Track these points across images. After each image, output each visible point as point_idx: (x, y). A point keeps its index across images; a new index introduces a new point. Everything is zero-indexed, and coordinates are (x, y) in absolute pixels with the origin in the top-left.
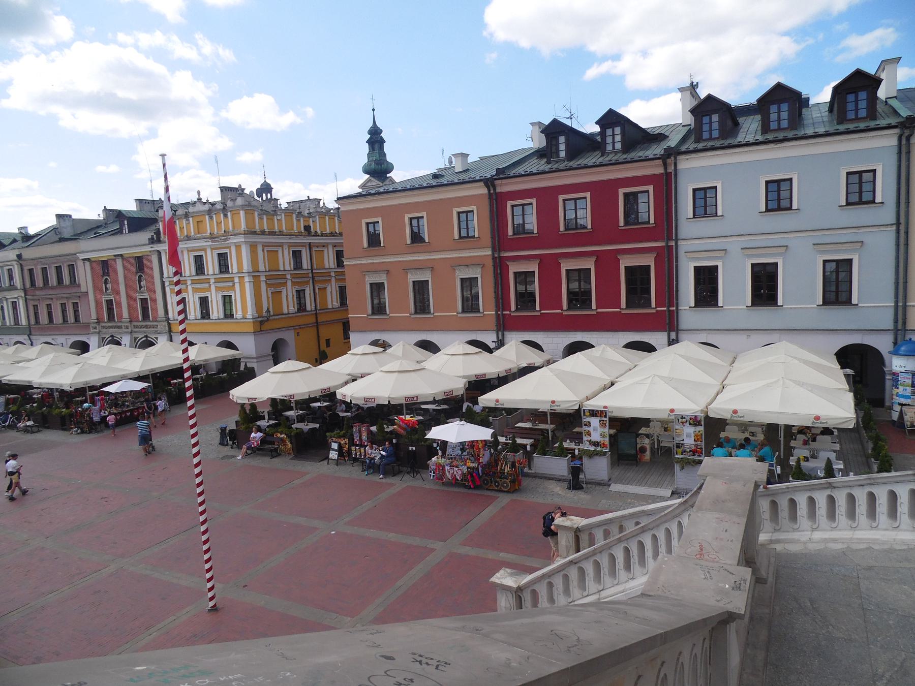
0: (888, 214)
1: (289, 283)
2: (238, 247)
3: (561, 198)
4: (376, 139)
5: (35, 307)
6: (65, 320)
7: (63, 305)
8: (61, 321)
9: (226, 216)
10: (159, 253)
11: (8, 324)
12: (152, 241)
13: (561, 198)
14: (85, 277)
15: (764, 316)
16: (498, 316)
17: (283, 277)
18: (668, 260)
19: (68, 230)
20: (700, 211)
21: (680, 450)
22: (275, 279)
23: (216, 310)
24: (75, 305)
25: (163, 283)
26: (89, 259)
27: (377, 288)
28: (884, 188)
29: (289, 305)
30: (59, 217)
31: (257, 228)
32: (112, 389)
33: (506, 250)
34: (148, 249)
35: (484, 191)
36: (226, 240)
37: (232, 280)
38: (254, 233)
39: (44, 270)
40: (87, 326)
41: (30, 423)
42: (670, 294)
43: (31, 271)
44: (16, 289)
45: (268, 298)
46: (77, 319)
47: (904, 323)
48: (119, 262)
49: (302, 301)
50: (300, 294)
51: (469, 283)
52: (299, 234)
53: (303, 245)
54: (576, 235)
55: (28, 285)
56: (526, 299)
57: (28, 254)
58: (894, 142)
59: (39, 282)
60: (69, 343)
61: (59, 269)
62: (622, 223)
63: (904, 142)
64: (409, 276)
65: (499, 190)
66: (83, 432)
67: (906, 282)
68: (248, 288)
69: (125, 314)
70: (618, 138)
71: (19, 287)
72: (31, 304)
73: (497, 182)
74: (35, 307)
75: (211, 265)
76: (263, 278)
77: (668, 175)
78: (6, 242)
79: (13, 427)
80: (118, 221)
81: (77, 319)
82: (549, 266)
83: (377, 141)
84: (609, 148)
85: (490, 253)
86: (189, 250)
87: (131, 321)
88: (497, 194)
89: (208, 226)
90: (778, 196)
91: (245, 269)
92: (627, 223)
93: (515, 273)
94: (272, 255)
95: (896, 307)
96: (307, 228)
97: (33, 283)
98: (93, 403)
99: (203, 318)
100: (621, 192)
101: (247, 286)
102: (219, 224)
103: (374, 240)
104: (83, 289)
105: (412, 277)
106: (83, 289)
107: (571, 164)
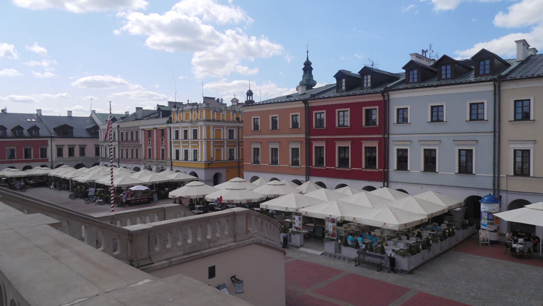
0: (489, 127)
1: (226, 146)
2: (201, 127)
3: (337, 110)
4: (308, 68)
5: (122, 149)
6: (132, 157)
7: (132, 149)
8: (131, 157)
9: (198, 112)
10: (170, 128)
13: (337, 110)
14: (142, 137)
15: (429, 177)
16: (306, 167)
17: (223, 142)
18: (385, 144)
19: (142, 115)
20: (401, 120)
21: (327, 234)
22: (218, 143)
23: (191, 157)
24: (137, 150)
25: (171, 142)
26: (144, 129)
28: (488, 112)
29: (224, 156)
30: (137, 108)
31: (211, 118)
32: (133, 189)
33: (311, 135)
34: (166, 126)
35: (303, 105)
36: (196, 123)
37: (197, 143)
38: (209, 121)
39: (127, 133)
40: (140, 160)
41: (101, 200)
42: (385, 163)
43: (122, 133)
44: (116, 141)
45: (214, 152)
46: (137, 157)
47: (498, 186)
48: (155, 131)
49: (232, 155)
50: (231, 151)
51: (295, 151)
52: (233, 122)
53: (235, 127)
54: (343, 130)
55: (120, 139)
56: (320, 161)
57: (122, 125)
58: (492, 88)
59: (124, 139)
60: (133, 167)
61: (132, 132)
62: (364, 124)
63: (497, 89)
64: (270, 146)
65: (310, 105)
66: (119, 206)
67: (499, 164)
68: (204, 146)
70: (369, 81)
72: (121, 148)
73: (309, 101)
74: (122, 149)
75: (190, 135)
76: (212, 143)
77: (384, 100)
78: (117, 118)
79: (94, 201)
80: (162, 112)
81: (137, 157)
82: (330, 144)
83: (308, 69)
84: (365, 85)
85: (304, 136)
86: (182, 128)
87: (157, 159)
88: (308, 107)
89: (191, 117)
90: (437, 115)
91: (203, 137)
92: (366, 124)
93: (366, 147)
94: (218, 132)
95: (494, 176)
96: (238, 119)
97: (122, 139)
98: (125, 194)
99: (185, 160)
100: (364, 108)
101: (204, 145)
102: (195, 115)
103: (256, 127)
104: (141, 143)
105: (272, 146)
106: (141, 143)
107: (348, 93)
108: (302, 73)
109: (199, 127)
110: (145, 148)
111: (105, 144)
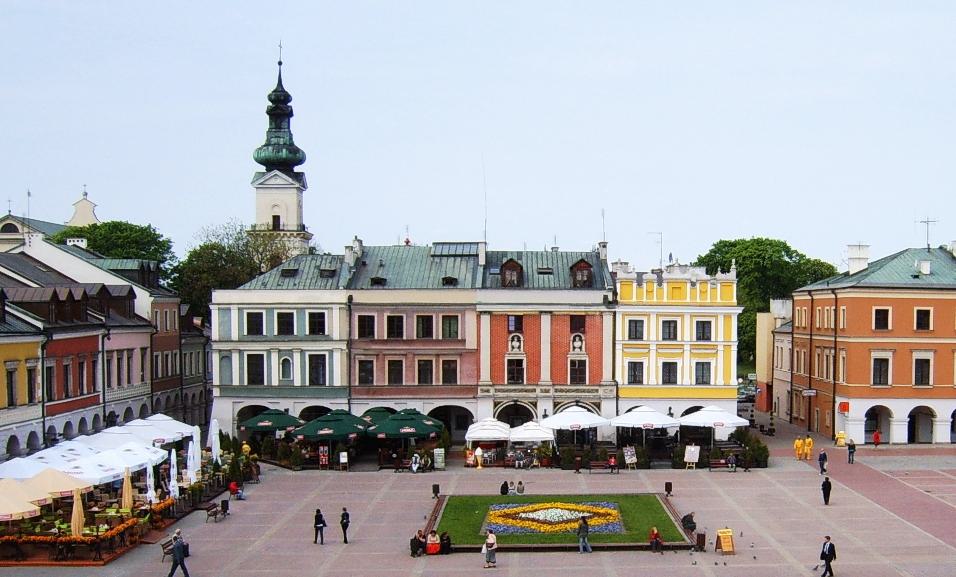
4: (280, 108)
10: (615, 313)
11: (297, 383)
12: (607, 302)
27: (881, 364)
48: (546, 321)
69: (545, 374)
71: (336, 336)
104: (471, 344)
106: (471, 344)
108: (265, 122)
109: (721, 319)
110: (495, 356)
111: (256, 348)
